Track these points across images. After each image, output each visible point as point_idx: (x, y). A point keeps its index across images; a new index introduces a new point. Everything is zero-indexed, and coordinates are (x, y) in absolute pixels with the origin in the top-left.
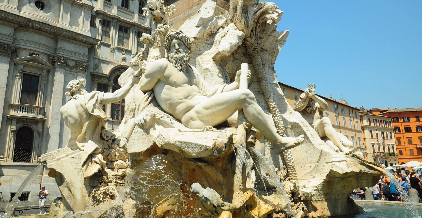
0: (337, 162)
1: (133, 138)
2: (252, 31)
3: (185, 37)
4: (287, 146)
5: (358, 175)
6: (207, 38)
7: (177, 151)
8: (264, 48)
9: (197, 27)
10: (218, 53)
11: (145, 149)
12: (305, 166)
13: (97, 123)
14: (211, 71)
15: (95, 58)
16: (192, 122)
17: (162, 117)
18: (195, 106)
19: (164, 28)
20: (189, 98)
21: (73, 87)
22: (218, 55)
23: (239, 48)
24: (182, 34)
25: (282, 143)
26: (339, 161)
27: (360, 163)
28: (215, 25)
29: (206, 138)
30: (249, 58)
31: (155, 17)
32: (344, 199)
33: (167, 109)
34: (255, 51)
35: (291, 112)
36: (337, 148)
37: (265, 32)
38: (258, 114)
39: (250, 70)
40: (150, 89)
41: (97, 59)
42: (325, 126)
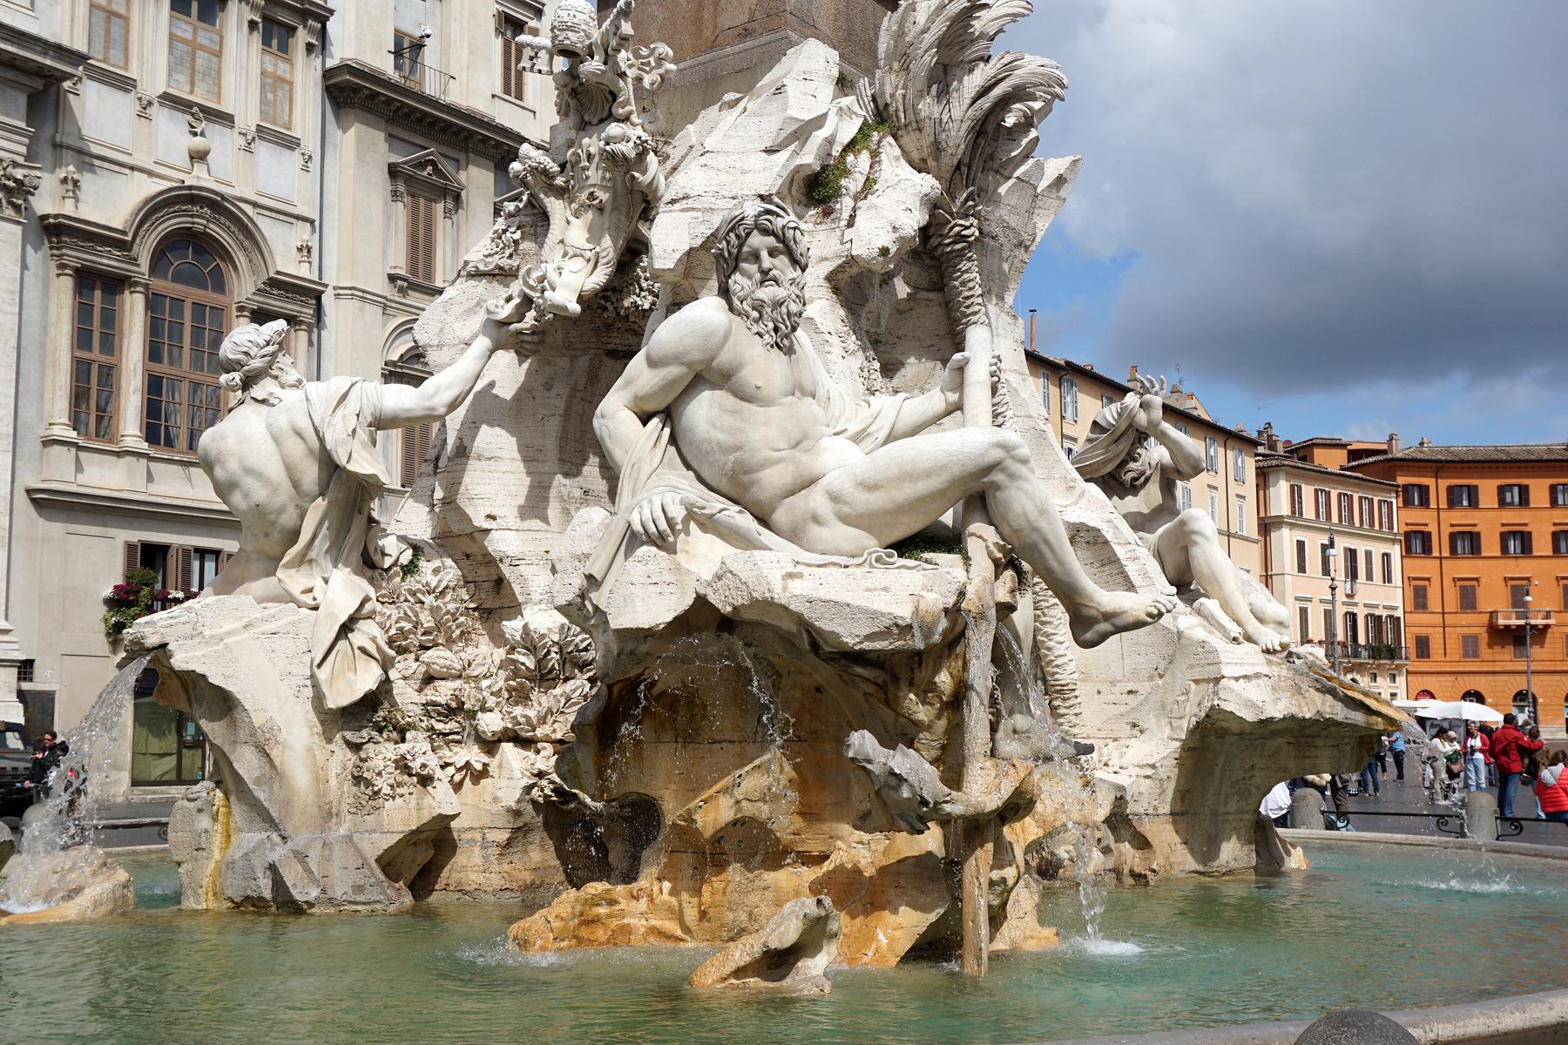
0: (1237, 679)
2: (958, 167)
3: (795, 228)
4: (1119, 621)
5: (1305, 727)
7: (788, 626)
9: (770, 151)
11: (669, 618)
12: (1113, 690)
13: (355, 503)
14: (822, 328)
19: (631, 144)
20: (805, 444)
21: (252, 354)
26: (1245, 677)
27: (1318, 686)
29: (886, 589)
30: (932, 271)
31: (581, 84)
32: (1247, 812)
33: (725, 481)
35: (1072, 484)
36: (1235, 630)
38: (1036, 513)
40: (662, 406)
41: (69, 148)
42: (1195, 543)
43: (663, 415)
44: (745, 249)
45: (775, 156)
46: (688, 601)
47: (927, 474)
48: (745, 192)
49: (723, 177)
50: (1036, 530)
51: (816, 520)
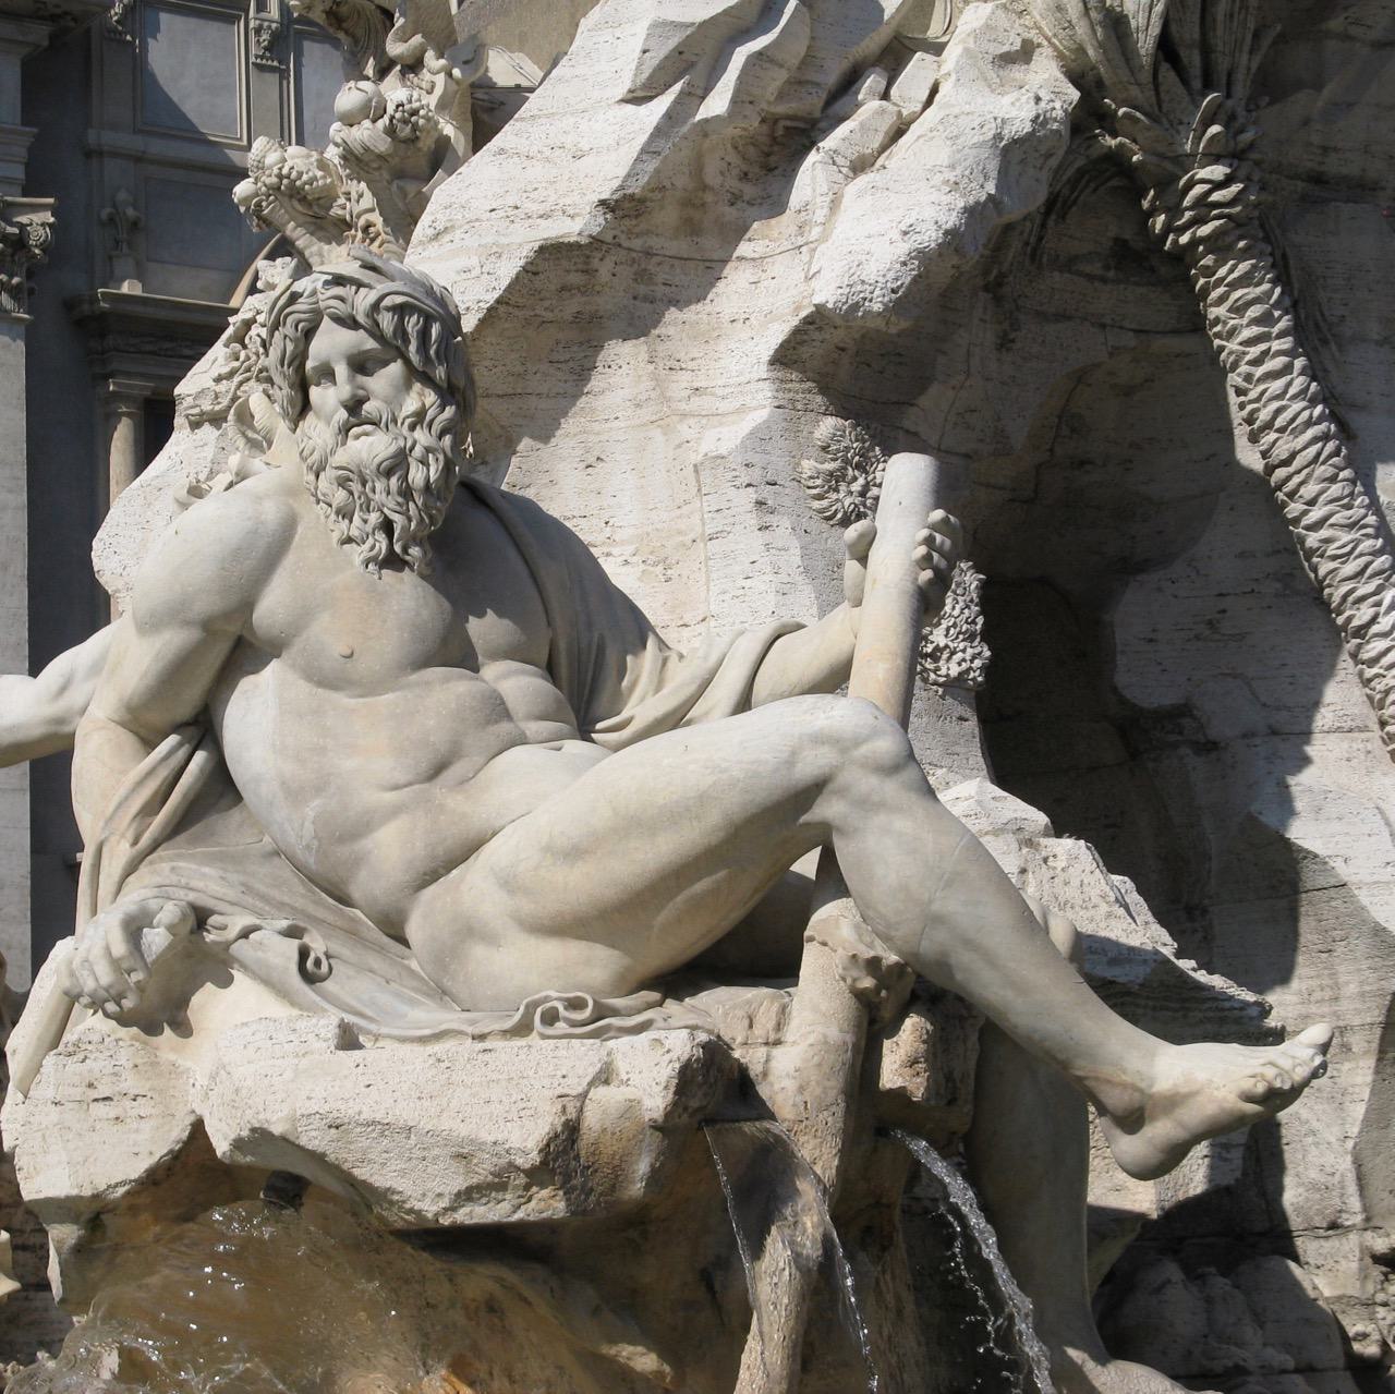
1: (50, 1094)
6: (733, 183)
8: (1333, 166)
9: (637, 98)
10: (809, 321)
11: (137, 1169)
15: (101, 154)
16: (479, 951)
17: (245, 934)
18: (494, 834)
22: (817, 335)
23: (1063, 217)
24: (382, 287)
25: (1155, 1089)
28: (795, 62)
34: (1205, 230)
37: (1335, 24)
39: (939, 514)
41: (115, 154)
43: (192, 731)
44: (309, 365)
45: (643, 109)
46: (178, 1132)
47: (672, 816)
48: (574, 198)
49: (537, 172)
50: (937, 920)
51: (470, 931)
